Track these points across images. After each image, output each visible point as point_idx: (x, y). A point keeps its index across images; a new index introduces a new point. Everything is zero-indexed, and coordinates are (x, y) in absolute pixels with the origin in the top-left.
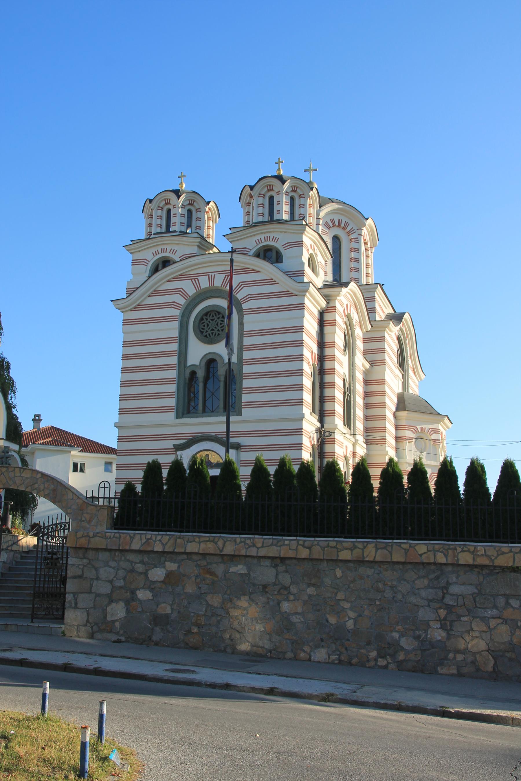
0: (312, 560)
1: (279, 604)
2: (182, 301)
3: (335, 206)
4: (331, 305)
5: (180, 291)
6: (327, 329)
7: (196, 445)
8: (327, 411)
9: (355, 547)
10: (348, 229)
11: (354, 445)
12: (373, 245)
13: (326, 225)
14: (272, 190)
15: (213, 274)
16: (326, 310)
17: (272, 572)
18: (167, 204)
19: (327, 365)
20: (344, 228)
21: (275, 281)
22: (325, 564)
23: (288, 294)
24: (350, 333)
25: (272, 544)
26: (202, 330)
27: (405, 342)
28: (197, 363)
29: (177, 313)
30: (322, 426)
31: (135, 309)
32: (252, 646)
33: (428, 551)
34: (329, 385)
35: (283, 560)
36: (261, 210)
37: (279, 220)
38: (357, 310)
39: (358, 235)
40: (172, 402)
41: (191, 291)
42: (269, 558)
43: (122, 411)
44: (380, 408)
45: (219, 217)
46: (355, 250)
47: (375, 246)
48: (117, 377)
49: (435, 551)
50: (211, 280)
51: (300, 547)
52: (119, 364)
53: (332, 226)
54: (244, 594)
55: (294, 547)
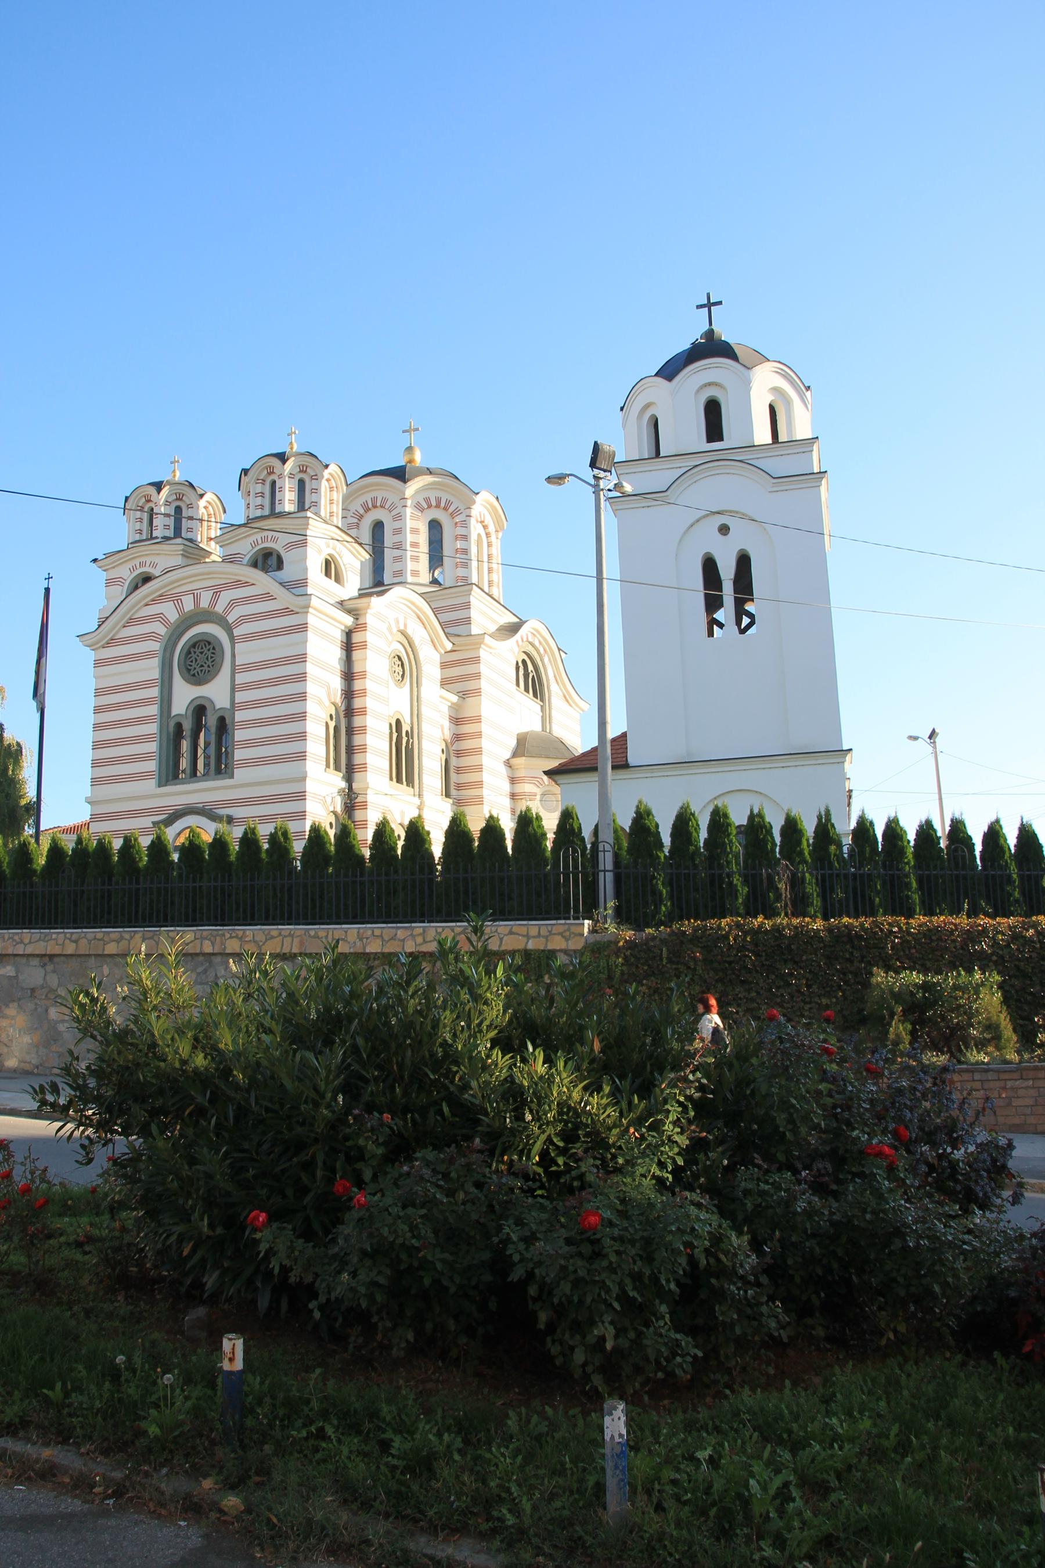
0: (80, 956)
1: (47, 1010)
2: (162, 630)
3: (429, 479)
4: (361, 621)
5: (160, 617)
6: (356, 655)
9: (122, 938)
10: (451, 510)
12: (499, 528)
13: (418, 507)
14: (273, 473)
17: (41, 972)
18: (149, 501)
19: (357, 703)
20: (445, 509)
22: (93, 960)
23: (288, 612)
24: (412, 657)
25: (40, 940)
27: (542, 660)
29: (156, 646)
30: (350, 788)
31: (107, 645)
32: (20, 1062)
33: (196, 939)
35: (51, 957)
36: (259, 501)
37: (280, 513)
40: (152, 766)
41: (173, 616)
42: (37, 956)
43: (95, 781)
45: (225, 512)
47: (502, 529)
48: (88, 737)
49: (203, 938)
50: (197, 601)
51: (67, 941)
52: (91, 719)
54: (13, 1001)
55: (60, 942)
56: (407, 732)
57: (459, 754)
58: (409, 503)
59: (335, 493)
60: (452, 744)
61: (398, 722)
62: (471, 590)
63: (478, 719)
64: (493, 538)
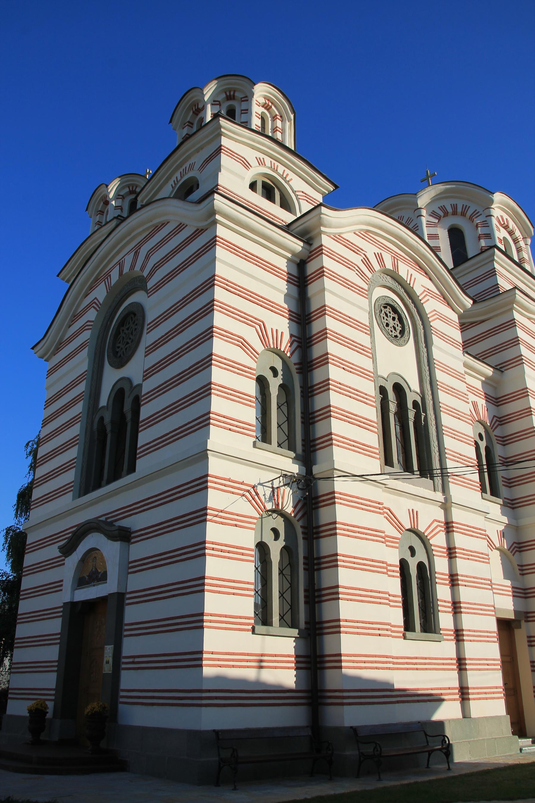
2: (92, 315)
4: (315, 245)
6: (312, 289)
7: (83, 541)
8: (320, 438)
10: (469, 214)
11: (446, 506)
13: (433, 214)
15: (123, 259)
16: (309, 257)
20: (463, 214)
21: (184, 225)
26: (117, 350)
28: (105, 404)
30: (309, 471)
31: (58, 349)
34: (320, 388)
38: (426, 273)
39: (486, 217)
44: (526, 438)
46: (485, 236)
53: (442, 214)
56: (415, 403)
57: (505, 441)
58: (424, 212)
59: (279, 123)
60: (494, 427)
61: (398, 389)
62: (494, 254)
63: (524, 393)
64: (522, 244)
